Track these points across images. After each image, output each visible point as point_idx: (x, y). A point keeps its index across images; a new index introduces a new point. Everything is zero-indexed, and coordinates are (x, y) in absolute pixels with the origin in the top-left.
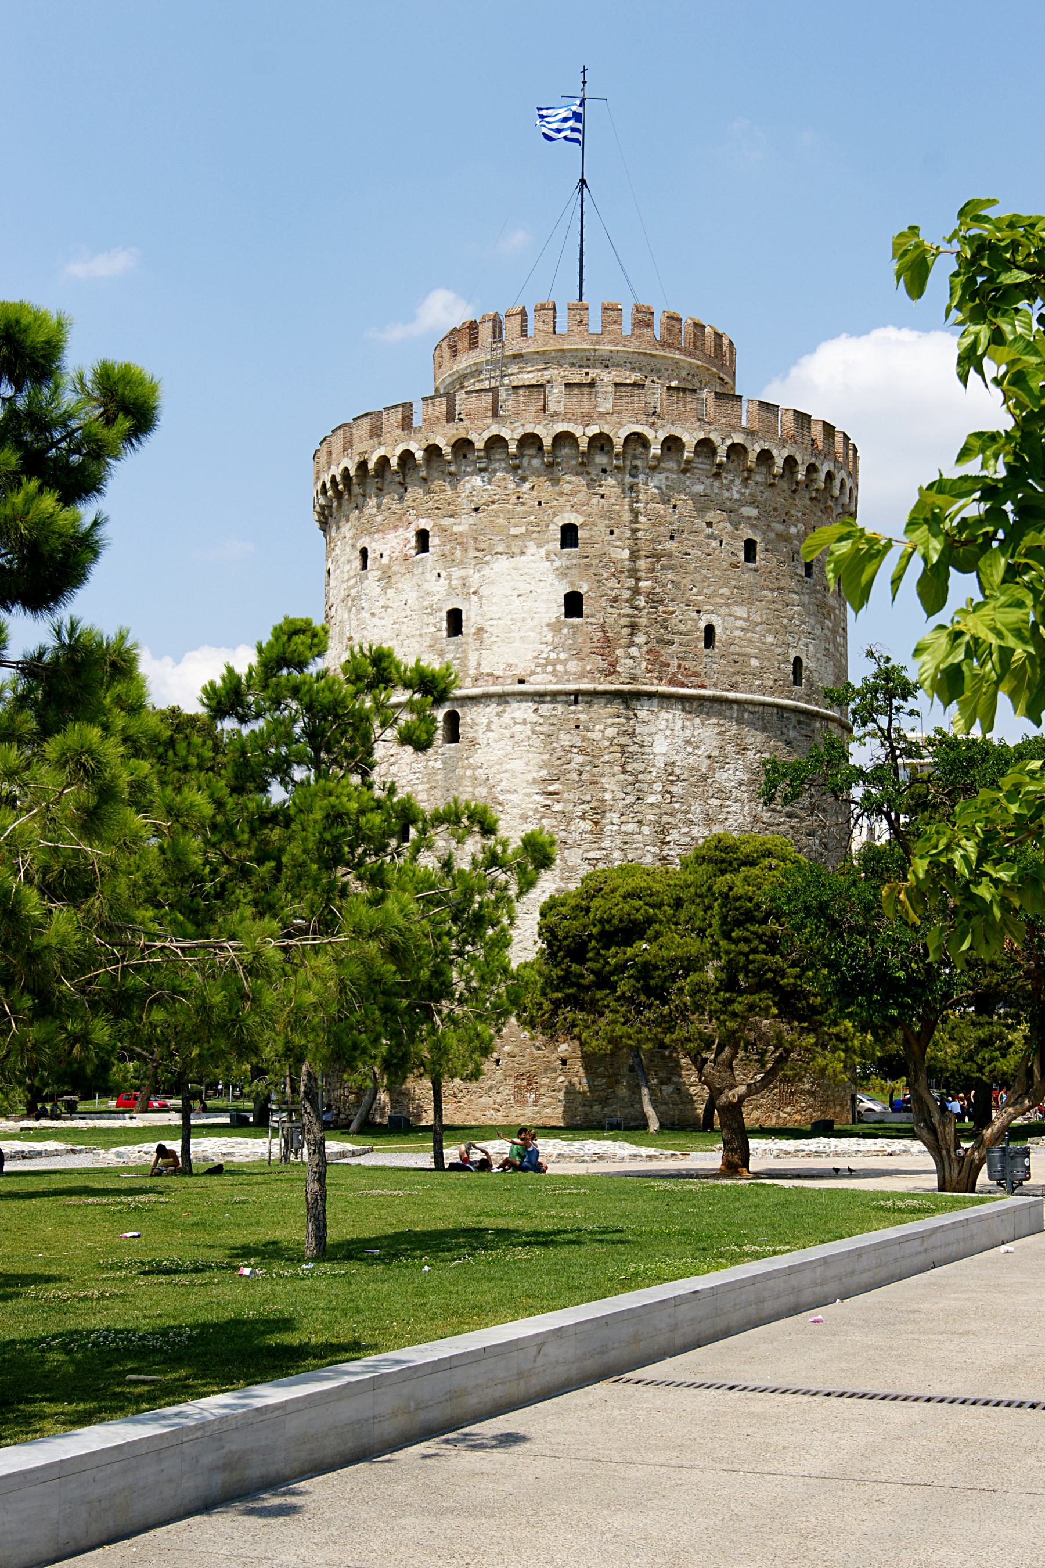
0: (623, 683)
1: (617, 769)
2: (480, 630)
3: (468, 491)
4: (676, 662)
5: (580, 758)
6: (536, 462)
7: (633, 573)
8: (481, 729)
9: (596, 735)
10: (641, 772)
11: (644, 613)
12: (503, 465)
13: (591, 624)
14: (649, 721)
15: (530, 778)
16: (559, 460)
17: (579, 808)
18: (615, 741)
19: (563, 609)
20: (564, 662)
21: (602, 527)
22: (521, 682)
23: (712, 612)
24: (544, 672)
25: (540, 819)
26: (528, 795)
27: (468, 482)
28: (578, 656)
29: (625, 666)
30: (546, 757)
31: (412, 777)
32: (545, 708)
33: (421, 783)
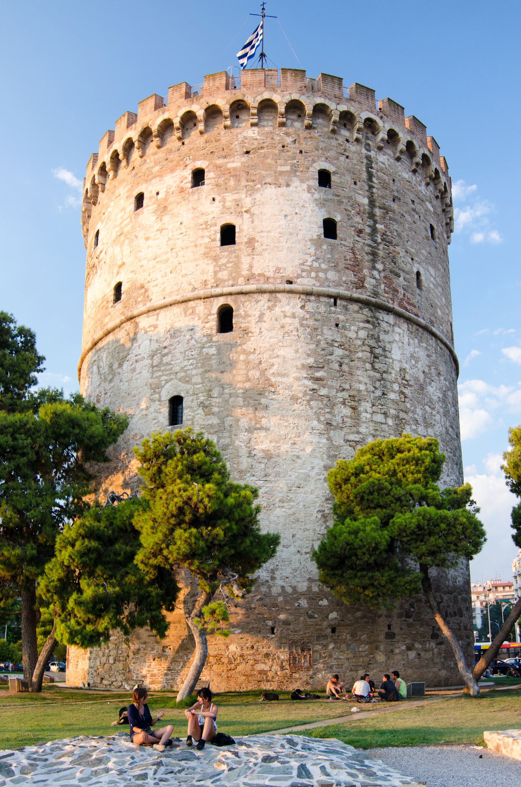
0: (369, 296)
3: (240, 140)
5: (339, 352)
6: (297, 125)
7: (372, 216)
9: (352, 335)
11: (381, 247)
12: (270, 123)
16: (315, 126)
17: (340, 395)
18: (366, 342)
21: (348, 178)
25: (309, 401)
27: (240, 133)
29: (369, 283)
31: (186, 363)
33: (195, 368)
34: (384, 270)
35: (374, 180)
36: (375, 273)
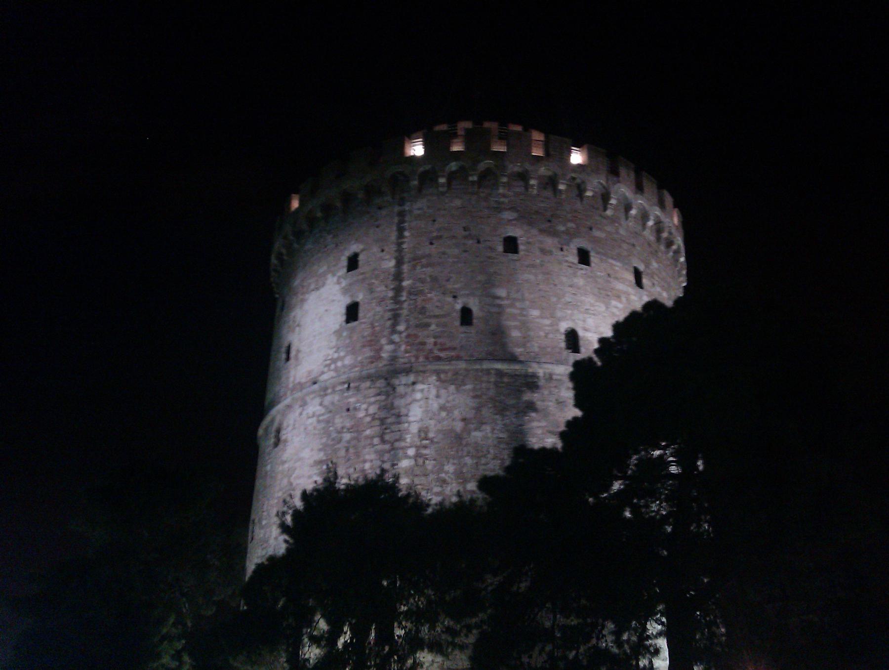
1: (376, 441)
2: (298, 351)
4: (432, 340)
8: (290, 428)
9: (361, 414)
10: (397, 440)
11: (405, 305)
13: (364, 323)
14: (406, 394)
15: (311, 461)
18: (377, 416)
19: (344, 318)
20: (340, 359)
22: (315, 383)
23: (468, 295)
24: (329, 370)
26: (310, 477)
28: (353, 352)
30: (324, 440)
32: (328, 400)
34: (407, 329)
35: (407, 234)
36: (396, 338)
